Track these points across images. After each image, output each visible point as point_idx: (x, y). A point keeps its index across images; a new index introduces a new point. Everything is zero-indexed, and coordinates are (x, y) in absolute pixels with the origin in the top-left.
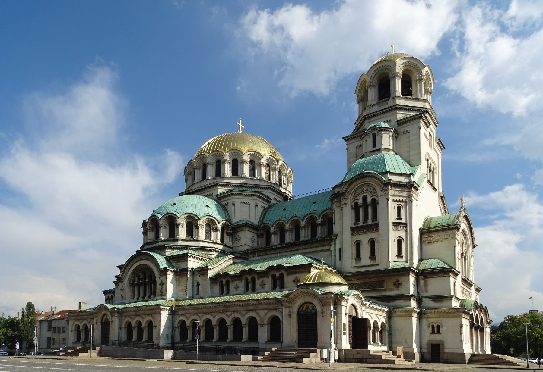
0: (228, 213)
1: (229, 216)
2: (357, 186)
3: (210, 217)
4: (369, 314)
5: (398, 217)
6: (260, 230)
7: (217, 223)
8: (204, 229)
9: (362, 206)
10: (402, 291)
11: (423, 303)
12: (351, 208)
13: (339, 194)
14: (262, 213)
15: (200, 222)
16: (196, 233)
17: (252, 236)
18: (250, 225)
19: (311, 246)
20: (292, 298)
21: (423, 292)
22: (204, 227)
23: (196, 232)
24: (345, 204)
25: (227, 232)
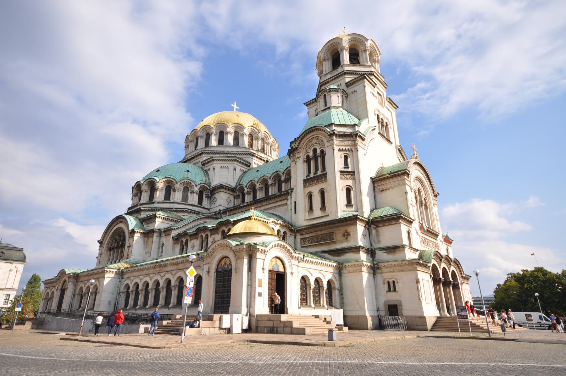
0: (209, 178)
1: (209, 180)
2: (308, 140)
3: (188, 181)
4: (307, 269)
5: (345, 166)
6: (236, 191)
7: (194, 186)
8: (182, 192)
9: (313, 158)
10: (351, 242)
11: (376, 255)
12: (304, 161)
13: (293, 149)
14: (240, 176)
15: (177, 186)
16: (173, 196)
17: (228, 197)
18: (225, 187)
19: (271, 202)
20: (211, 253)
21: (376, 243)
22: (182, 190)
23: (173, 194)
24: (298, 158)
25: (205, 194)
